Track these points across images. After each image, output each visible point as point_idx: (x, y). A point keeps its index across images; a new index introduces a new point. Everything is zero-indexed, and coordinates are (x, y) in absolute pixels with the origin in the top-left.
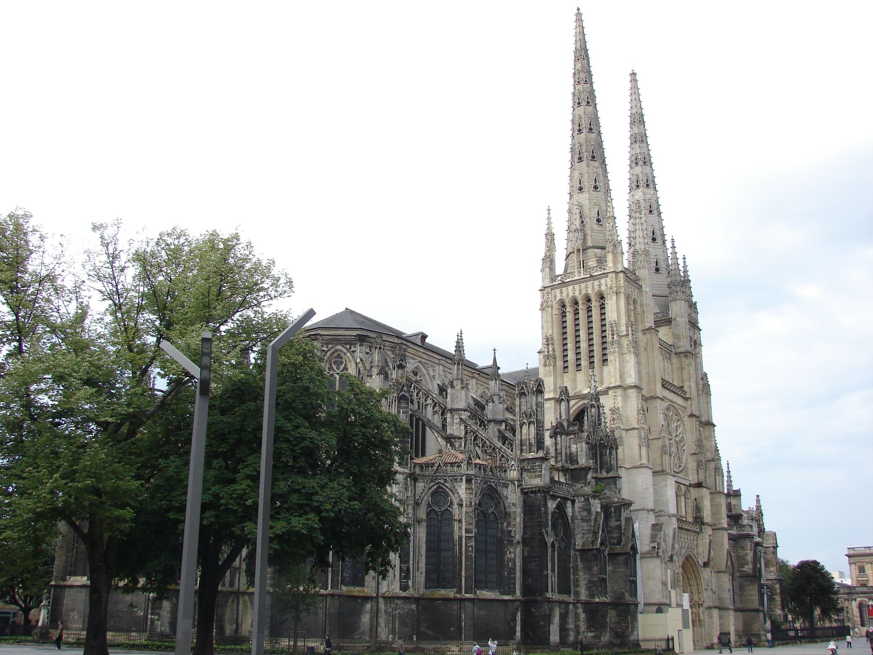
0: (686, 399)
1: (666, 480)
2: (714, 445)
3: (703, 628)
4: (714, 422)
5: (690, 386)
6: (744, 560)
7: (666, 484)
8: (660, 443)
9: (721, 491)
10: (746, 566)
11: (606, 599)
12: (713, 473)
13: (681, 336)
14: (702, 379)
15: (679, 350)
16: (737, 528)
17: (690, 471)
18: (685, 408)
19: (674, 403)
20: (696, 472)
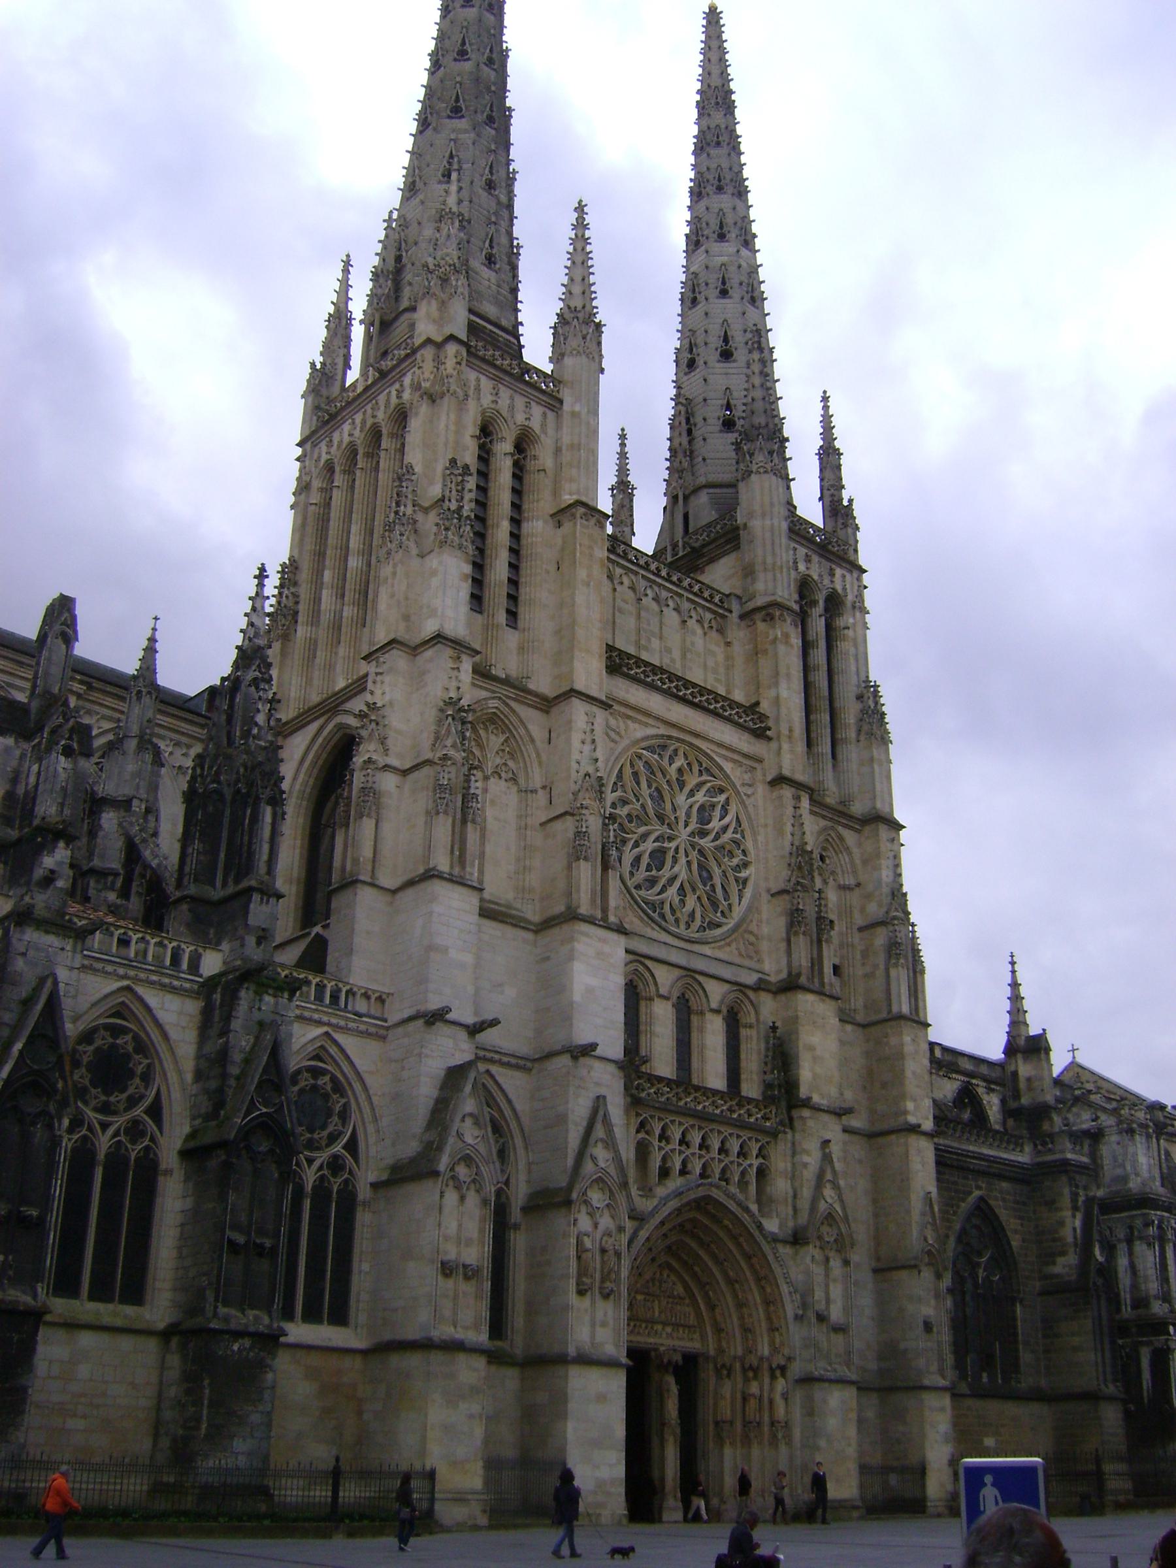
0: (760, 734)
1: (572, 939)
2: (886, 875)
3: (783, 1449)
4: (899, 815)
5: (777, 701)
6: (1054, 1240)
7: (572, 950)
8: (569, 824)
9: (905, 1009)
10: (1061, 1260)
11: (33, 1302)
12: (881, 959)
13: (758, 568)
14: (860, 697)
15: (751, 605)
16: (1035, 1145)
17: (764, 946)
18: (760, 761)
19: (697, 735)
20: (783, 945)
